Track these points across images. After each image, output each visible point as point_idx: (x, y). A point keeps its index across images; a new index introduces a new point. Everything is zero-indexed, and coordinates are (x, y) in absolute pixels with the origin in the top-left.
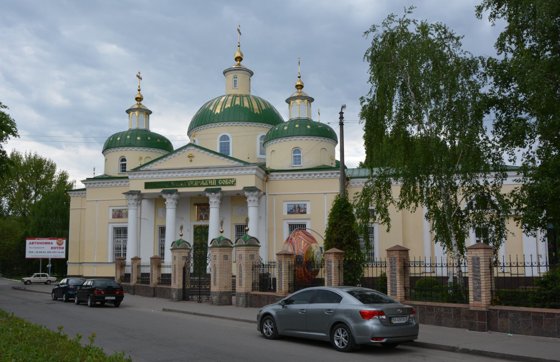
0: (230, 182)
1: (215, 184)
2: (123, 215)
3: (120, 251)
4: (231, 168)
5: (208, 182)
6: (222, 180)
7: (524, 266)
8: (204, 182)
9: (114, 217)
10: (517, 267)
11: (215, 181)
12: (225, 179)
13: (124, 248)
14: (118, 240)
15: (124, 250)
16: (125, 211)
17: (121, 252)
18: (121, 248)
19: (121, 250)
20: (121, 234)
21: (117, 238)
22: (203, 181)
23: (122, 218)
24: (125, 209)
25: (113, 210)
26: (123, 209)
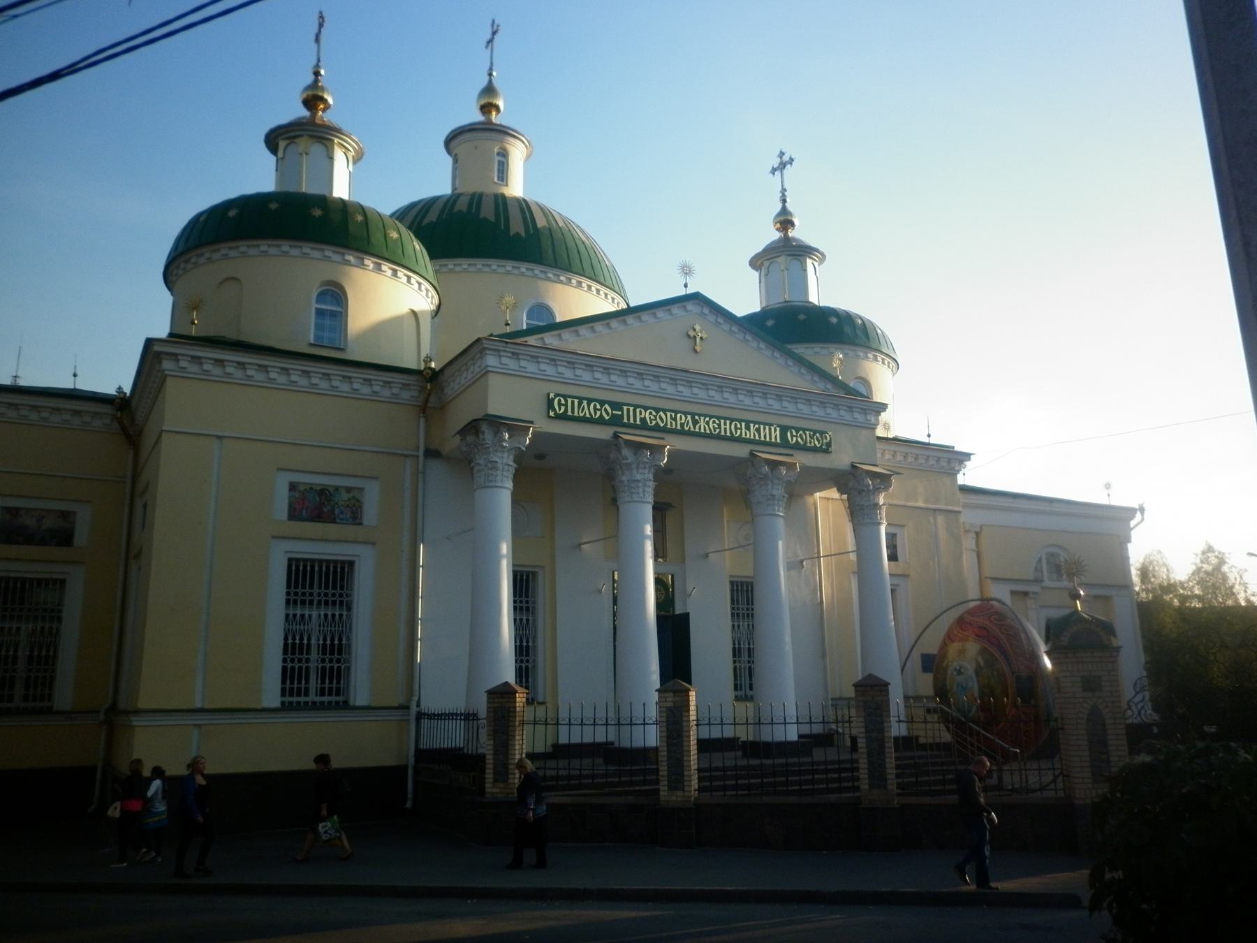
0: (802, 439)
1: (778, 441)
2: (337, 511)
3: (308, 660)
4: (823, 400)
5: (758, 430)
6: (797, 430)
7: (557, 724)
8: (748, 428)
9: (294, 515)
10: (568, 726)
11: (778, 429)
12: (804, 430)
13: (324, 645)
14: (307, 613)
15: (324, 653)
16: (345, 496)
17: (313, 665)
18: (309, 645)
19: (308, 653)
20: (311, 587)
21: (303, 603)
22: (743, 424)
23: (334, 522)
24: (349, 490)
25: (293, 487)
26: (337, 489)
